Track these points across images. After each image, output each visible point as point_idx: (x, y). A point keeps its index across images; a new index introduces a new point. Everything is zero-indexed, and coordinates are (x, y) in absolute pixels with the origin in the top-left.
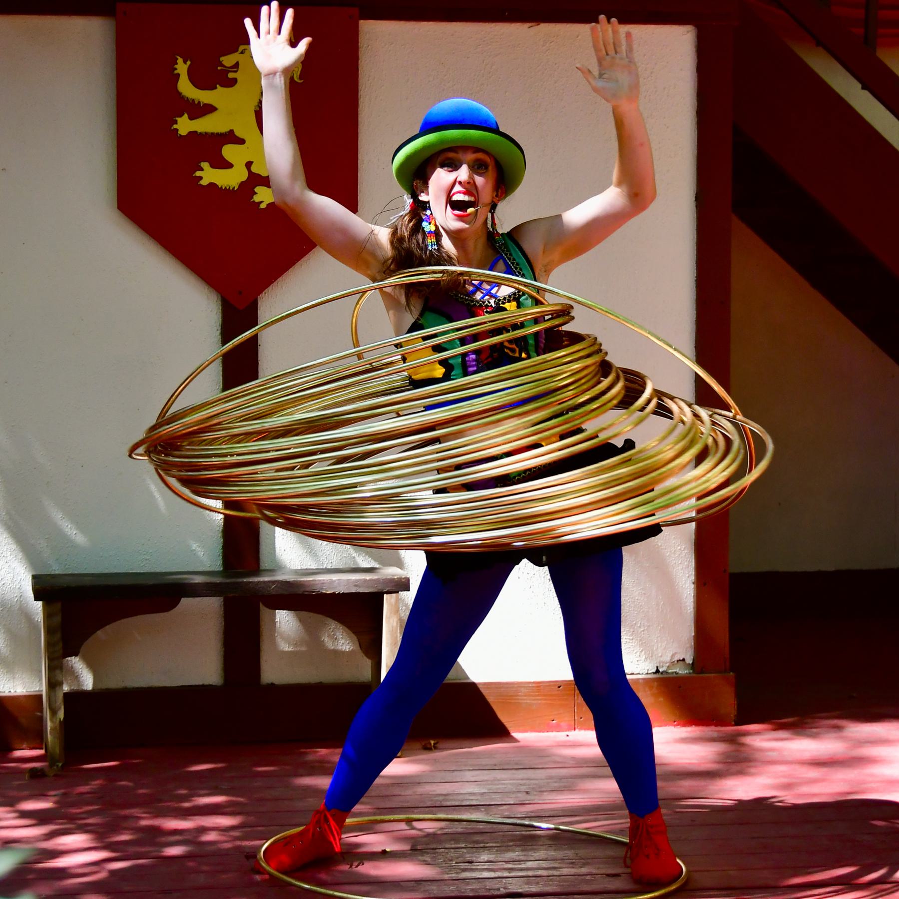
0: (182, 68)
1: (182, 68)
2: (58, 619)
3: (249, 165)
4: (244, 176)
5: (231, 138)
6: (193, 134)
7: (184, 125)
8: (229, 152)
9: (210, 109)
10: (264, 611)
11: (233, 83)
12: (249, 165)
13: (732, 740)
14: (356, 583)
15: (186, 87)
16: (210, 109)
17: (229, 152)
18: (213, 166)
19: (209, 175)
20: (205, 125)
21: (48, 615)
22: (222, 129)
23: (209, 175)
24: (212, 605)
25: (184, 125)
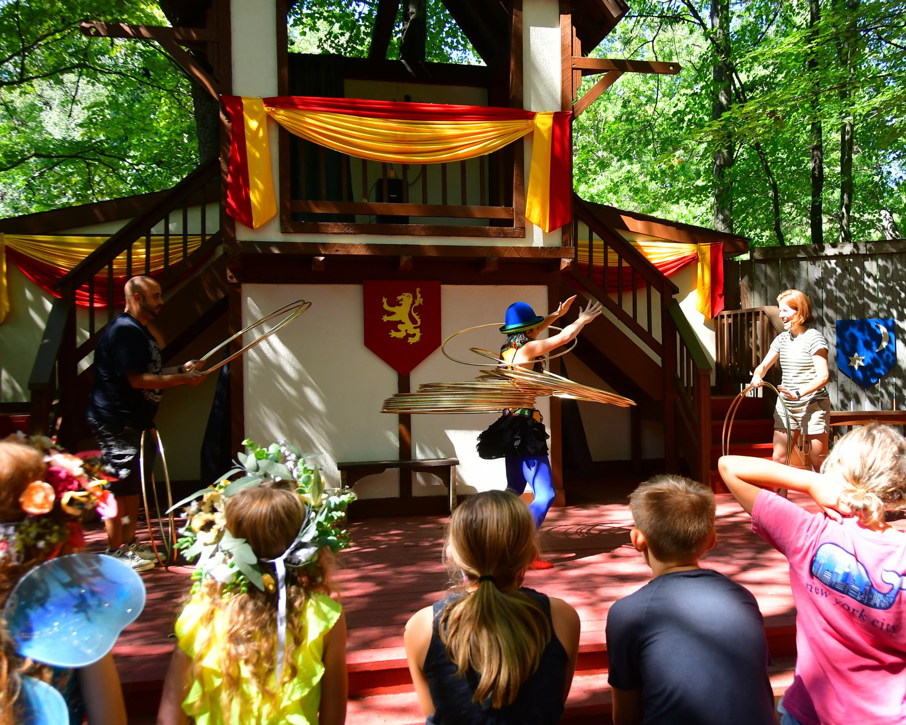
0: (385, 300)
1: (385, 300)
2: (345, 476)
3: (406, 331)
4: (405, 334)
5: (401, 322)
6: (388, 321)
7: (386, 318)
8: (400, 326)
9: (394, 313)
10: (413, 472)
11: (401, 305)
12: (406, 331)
13: (563, 511)
14: (442, 462)
15: (386, 307)
16: (394, 313)
17: (400, 326)
18: (395, 331)
19: (393, 334)
20: (392, 318)
21: (342, 475)
22: (398, 319)
23: (393, 334)
24: (396, 471)
25: (386, 318)
